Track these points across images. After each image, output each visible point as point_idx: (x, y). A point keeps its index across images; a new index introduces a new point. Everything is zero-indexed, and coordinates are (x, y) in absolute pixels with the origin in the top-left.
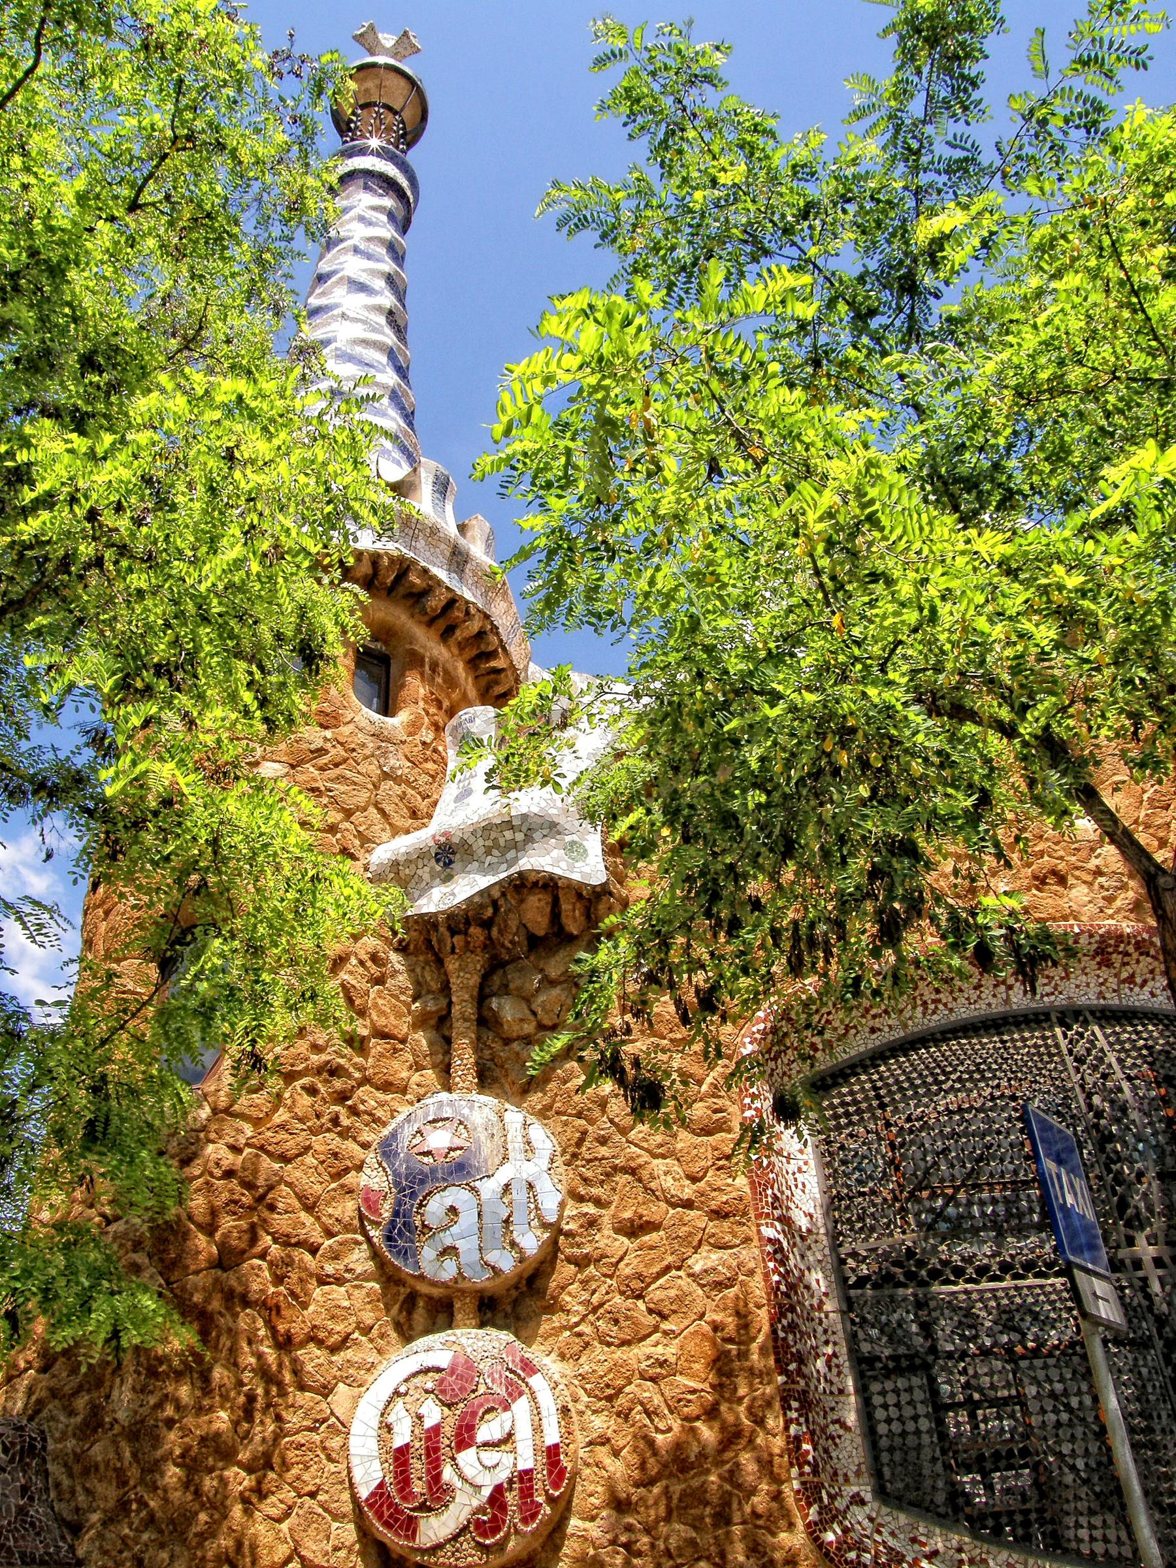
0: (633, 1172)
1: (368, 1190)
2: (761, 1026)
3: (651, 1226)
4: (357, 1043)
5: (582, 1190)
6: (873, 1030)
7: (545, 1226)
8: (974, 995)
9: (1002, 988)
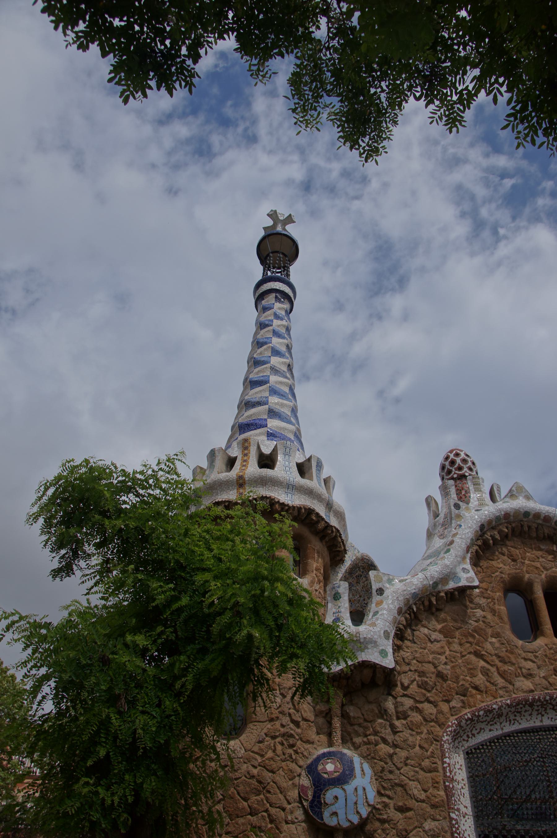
0: (402, 786)
1: (303, 786)
2: (450, 729)
3: (409, 809)
4: (297, 724)
5: (383, 792)
6: (490, 730)
7: (369, 805)
8: (529, 718)
9: (540, 715)
